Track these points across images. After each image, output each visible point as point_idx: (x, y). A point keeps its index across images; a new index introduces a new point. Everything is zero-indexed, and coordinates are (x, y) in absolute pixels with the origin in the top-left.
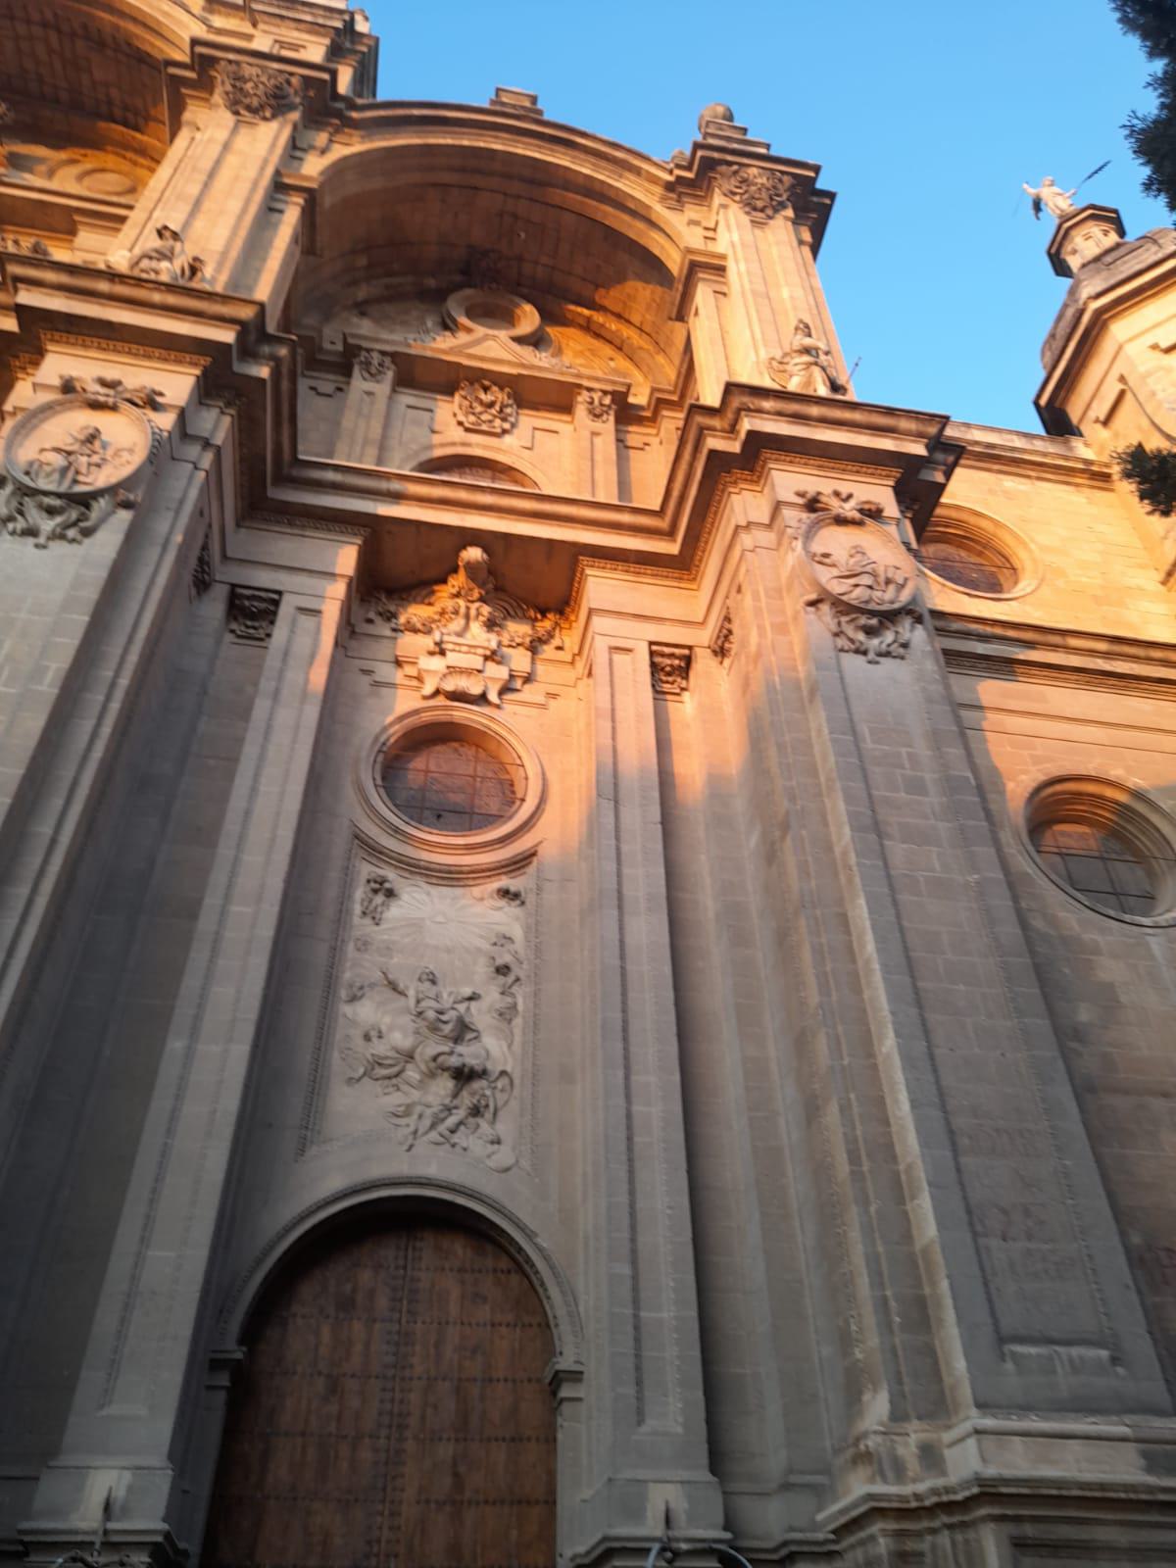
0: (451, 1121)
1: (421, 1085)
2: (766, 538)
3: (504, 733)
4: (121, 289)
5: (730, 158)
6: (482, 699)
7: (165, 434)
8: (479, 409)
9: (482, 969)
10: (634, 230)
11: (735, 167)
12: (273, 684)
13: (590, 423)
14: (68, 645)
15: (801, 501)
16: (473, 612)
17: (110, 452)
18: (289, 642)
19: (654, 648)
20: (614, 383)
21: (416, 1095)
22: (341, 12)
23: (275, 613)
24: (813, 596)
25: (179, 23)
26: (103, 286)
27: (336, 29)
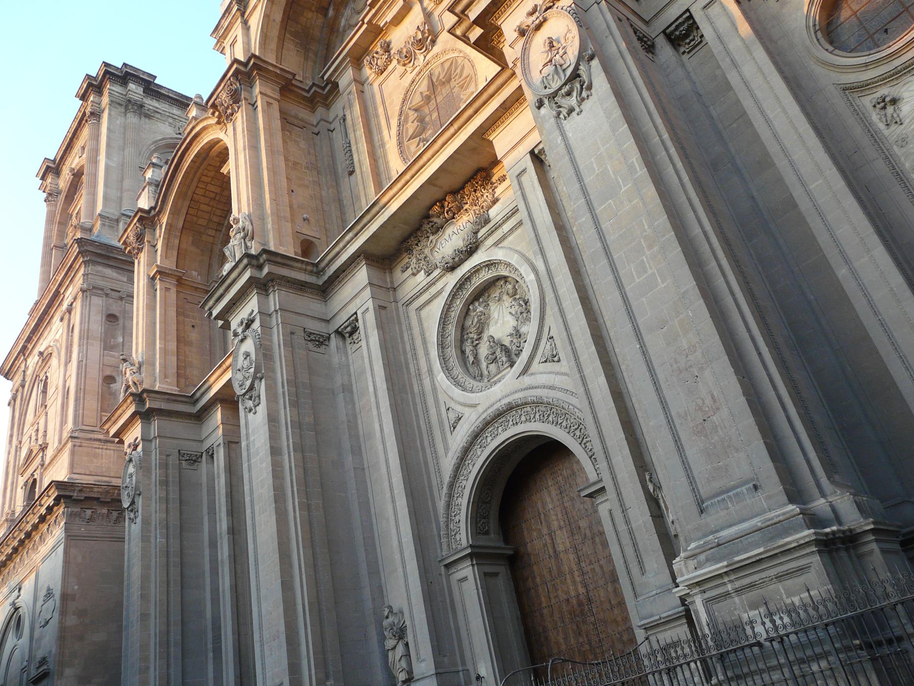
7: (573, 5)
12: (728, 59)
14: (630, 143)
17: (563, 41)
18: (715, 30)
23: (695, 22)
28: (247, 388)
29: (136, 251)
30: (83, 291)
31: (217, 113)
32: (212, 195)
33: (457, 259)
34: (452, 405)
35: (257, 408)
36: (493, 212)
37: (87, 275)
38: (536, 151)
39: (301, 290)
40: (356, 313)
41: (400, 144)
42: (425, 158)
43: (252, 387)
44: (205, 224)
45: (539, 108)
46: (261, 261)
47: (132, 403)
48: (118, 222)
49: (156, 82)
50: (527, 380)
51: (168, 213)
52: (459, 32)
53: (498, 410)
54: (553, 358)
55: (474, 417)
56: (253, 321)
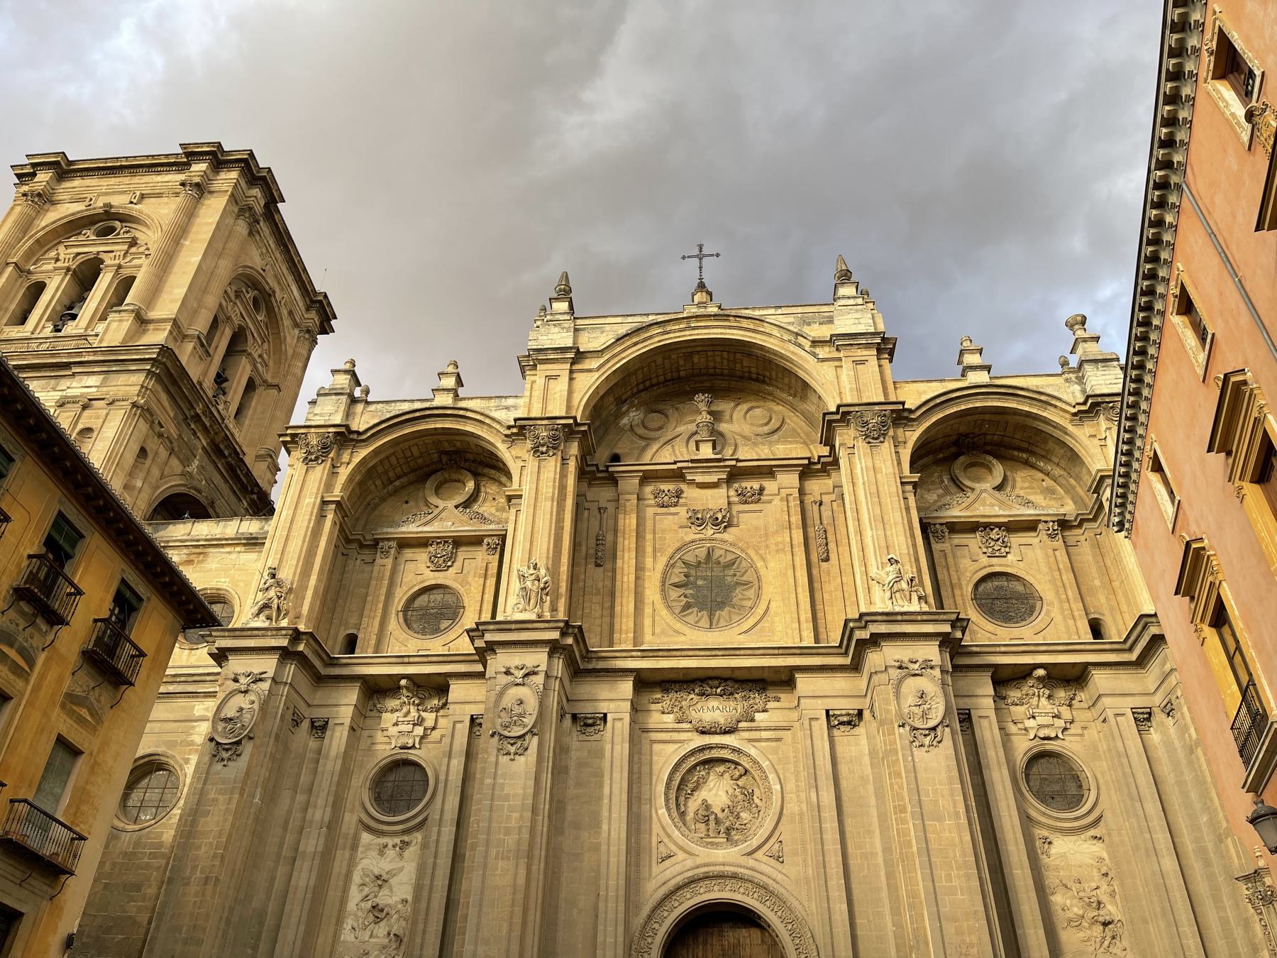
1: (1090, 928)
3: (1071, 754)
8: (993, 543)
9: (1096, 875)
10: (1057, 434)
11: (1111, 405)
16: (1041, 694)
19: (1134, 710)
20: (1057, 515)
21: (1089, 932)
25: (801, 357)
26: (899, 618)
28: (512, 734)
29: (313, 457)
30: (134, 405)
31: (515, 430)
32: (409, 454)
34: (666, 840)
35: (517, 756)
36: (758, 716)
37: (147, 389)
38: (831, 713)
39: (569, 665)
40: (605, 715)
41: (663, 583)
42: (742, 652)
43: (522, 737)
44: (380, 471)
45: (900, 726)
46: (570, 631)
47: (286, 635)
48: (183, 339)
50: (750, 862)
51: (371, 449)
52: (851, 624)
53: (723, 872)
54: (779, 858)
55: (689, 863)
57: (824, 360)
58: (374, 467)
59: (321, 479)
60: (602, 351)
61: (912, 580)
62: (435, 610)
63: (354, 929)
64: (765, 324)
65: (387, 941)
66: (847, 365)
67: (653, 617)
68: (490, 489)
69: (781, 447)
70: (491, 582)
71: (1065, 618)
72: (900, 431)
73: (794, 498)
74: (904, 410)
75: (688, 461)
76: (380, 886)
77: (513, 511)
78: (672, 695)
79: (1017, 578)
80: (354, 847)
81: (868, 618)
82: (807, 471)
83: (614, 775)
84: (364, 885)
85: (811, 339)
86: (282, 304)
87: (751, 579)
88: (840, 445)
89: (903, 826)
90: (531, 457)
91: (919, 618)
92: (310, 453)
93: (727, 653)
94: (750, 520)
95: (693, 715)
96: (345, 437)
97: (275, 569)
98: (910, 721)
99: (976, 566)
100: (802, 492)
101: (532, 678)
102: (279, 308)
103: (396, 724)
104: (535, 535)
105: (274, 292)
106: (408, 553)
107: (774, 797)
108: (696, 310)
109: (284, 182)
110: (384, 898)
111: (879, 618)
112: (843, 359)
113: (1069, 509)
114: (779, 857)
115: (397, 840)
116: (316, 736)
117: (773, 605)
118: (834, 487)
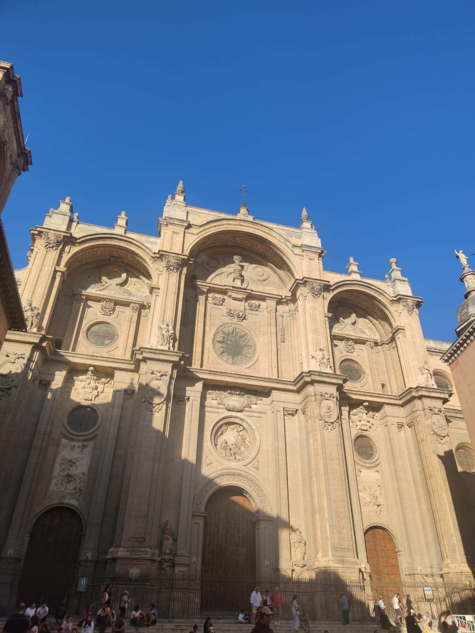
0: (378, 513)
1: (372, 507)
2: (422, 413)
3: (371, 437)
4: (326, 375)
5: (405, 297)
6: (367, 430)
8: (349, 346)
11: (406, 300)
13: (370, 350)
15: (429, 408)
16: (364, 412)
20: (375, 339)
22: (320, 248)
24: (433, 433)
26: (324, 375)
27: (319, 253)
29: (51, 246)
31: (158, 255)
33: (234, 409)
36: (253, 406)
38: (285, 409)
40: (189, 397)
41: (213, 341)
42: (253, 378)
43: (159, 404)
45: (320, 420)
49: (18, 97)
52: (304, 374)
53: (235, 472)
54: (257, 469)
55: (220, 468)
56: (166, 375)
57: (296, 255)
58: (79, 256)
59: (55, 258)
60: (201, 226)
61: (328, 359)
62: (103, 334)
63: (56, 484)
64: (273, 232)
65: (74, 492)
66: (306, 259)
67: (208, 354)
68: (132, 280)
69: (268, 288)
70: (134, 326)
71: (373, 383)
72: (325, 293)
73: (273, 312)
74: (329, 285)
75: (230, 286)
76: (71, 466)
77: (154, 295)
78: (217, 392)
79: (356, 362)
80: (58, 445)
81: (312, 373)
82: (280, 302)
83: (192, 425)
84: (62, 464)
85: (292, 244)
86: (9, 150)
87: (251, 345)
88: (300, 295)
89: (318, 462)
90: (165, 271)
91: (332, 376)
92: (49, 243)
93: (246, 377)
94: (251, 317)
95: (225, 401)
96: (69, 240)
97: (32, 301)
98: (324, 418)
99: (341, 355)
100: (276, 311)
101: (164, 377)
102: (7, 153)
103: (84, 388)
104: (166, 309)
105: (7, 144)
106: (89, 303)
107: (257, 442)
108: (243, 217)
109: (25, 88)
110: (73, 471)
111: (316, 373)
112: (305, 256)
113: (377, 337)
114: (257, 468)
115: (81, 444)
116: (42, 388)
117: (260, 358)
118: (290, 311)
